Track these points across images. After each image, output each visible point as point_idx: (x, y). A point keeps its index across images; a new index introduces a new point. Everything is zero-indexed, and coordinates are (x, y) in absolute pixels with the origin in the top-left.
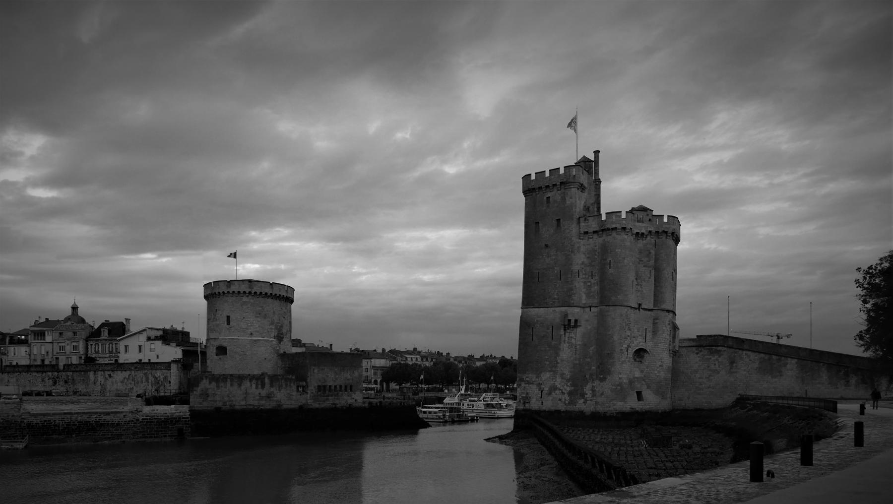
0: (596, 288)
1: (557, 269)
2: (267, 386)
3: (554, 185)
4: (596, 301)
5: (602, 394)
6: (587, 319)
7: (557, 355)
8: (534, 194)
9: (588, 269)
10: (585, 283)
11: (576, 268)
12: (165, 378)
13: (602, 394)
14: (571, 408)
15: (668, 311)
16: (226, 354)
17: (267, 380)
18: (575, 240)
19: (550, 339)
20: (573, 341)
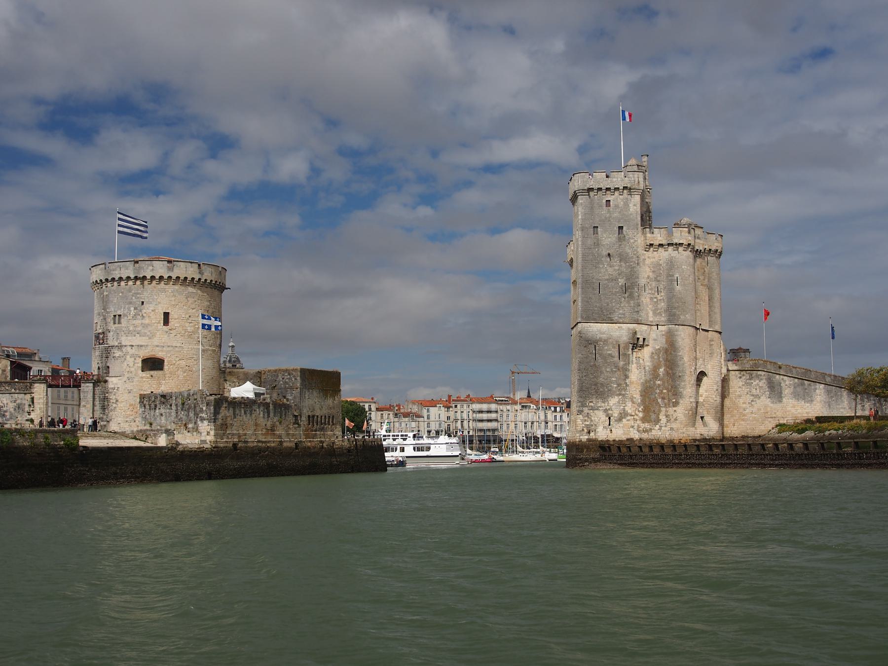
0: (663, 305)
1: (621, 281)
2: (272, 414)
3: (617, 189)
4: (663, 319)
5: (676, 420)
6: (655, 338)
7: (627, 377)
8: (592, 194)
9: (654, 284)
10: (651, 299)
11: (642, 281)
12: (19, 407)
13: (676, 420)
14: (645, 436)
15: (720, 333)
16: (161, 369)
17: (271, 407)
18: (641, 251)
19: (616, 359)
20: (641, 361)
